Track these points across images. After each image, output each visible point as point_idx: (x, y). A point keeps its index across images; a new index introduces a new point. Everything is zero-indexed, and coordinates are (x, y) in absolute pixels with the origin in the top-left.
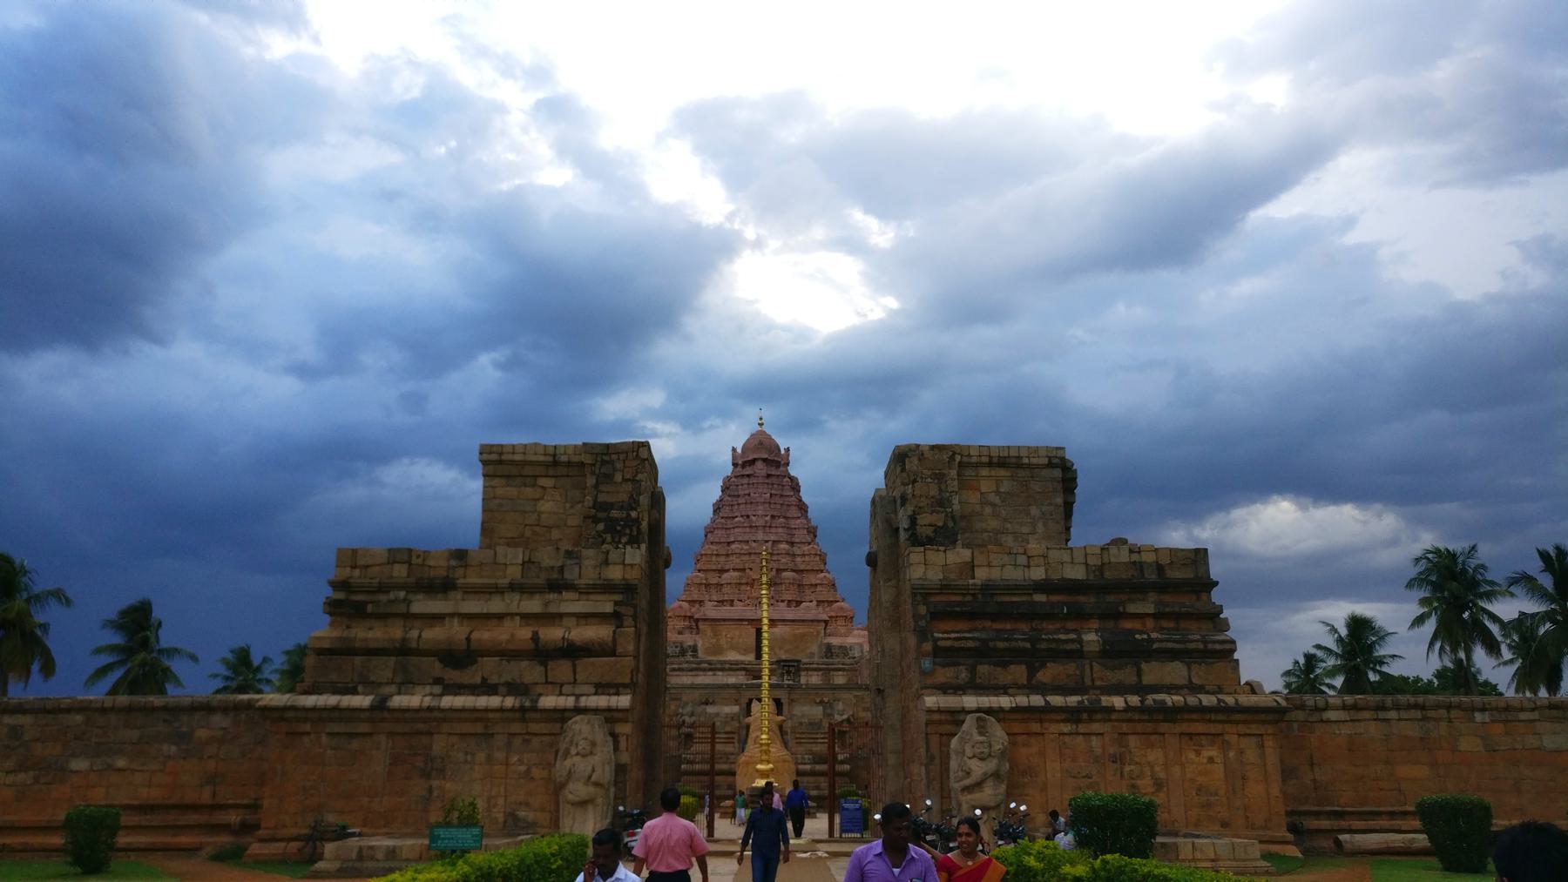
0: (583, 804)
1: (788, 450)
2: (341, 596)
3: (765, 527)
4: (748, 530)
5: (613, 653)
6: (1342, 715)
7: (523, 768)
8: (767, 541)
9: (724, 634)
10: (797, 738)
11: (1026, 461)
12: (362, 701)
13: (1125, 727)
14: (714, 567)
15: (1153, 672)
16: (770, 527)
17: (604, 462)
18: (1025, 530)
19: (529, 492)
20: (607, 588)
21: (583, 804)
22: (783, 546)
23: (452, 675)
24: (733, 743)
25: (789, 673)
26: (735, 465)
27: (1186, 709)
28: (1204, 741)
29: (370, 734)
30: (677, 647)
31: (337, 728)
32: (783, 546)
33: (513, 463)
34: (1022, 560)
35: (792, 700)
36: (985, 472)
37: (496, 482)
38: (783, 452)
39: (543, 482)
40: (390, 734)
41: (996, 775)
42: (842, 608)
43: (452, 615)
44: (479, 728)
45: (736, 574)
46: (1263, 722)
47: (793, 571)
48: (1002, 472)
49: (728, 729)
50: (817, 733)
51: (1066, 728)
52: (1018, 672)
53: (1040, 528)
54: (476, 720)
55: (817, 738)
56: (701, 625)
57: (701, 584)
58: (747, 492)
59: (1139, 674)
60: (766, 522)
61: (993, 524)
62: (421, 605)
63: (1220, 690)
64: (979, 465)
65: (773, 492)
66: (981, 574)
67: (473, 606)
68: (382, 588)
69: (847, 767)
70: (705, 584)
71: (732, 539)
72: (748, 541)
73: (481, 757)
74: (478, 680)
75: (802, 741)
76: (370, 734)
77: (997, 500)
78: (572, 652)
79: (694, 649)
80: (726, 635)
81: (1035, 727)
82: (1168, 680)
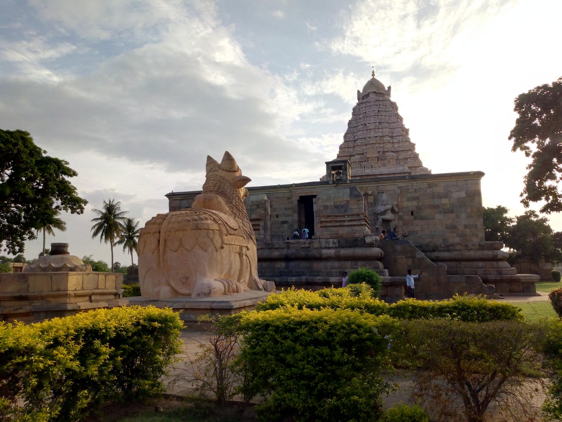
10: (321, 222)
16: (378, 129)
24: (259, 230)
26: (359, 99)
38: (387, 89)
50: (344, 216)
55: (344, 221)
58: (364, 111)
69: (376, 251)
71: (356, 138)
75: (328, 224)
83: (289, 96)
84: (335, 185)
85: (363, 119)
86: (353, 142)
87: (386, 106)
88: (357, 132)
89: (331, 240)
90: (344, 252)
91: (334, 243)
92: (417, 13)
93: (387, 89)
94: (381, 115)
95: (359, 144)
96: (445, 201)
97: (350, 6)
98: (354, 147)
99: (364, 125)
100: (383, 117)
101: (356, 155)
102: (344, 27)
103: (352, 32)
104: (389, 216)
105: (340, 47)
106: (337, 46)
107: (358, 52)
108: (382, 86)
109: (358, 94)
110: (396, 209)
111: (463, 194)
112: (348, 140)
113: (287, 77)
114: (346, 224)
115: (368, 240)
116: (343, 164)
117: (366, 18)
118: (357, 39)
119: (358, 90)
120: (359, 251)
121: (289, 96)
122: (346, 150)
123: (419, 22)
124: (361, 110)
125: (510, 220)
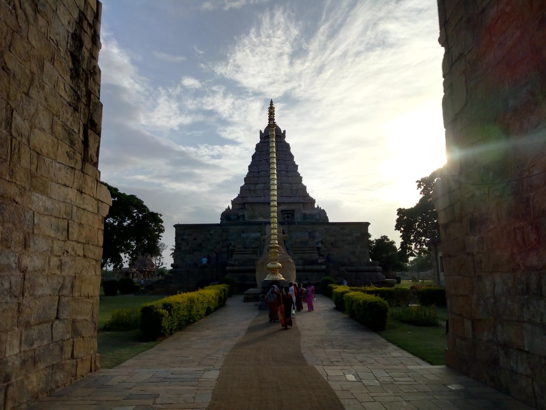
1: (285, 131)
14: (252, 182)
25: (288, 217)
26: (261, 138)
30: (235, 216)
35: (290, 231)
38: (282, 132)
49: (254, 246)
55: (305, 250)
56: (246, 206)
57: (246, 190)
58: (266, 149)
69: (324, 267)
70: (249, 190)
71: (260, 170)
72: (267, 171)
75: (298, 252)
79: (243, 216)
80: (258, 210)
83: (170, 108)
84: (289, 225)
85: (265, 155)
86: (257, 172)
87: (283, 146)
88: (261, 165)
89: (299, 261)
90: (307, 267)
91: (301, 263)
92: (291, 53)
93: (282, 132)
94: (279, 154)
95: (262, 175)
96: (349, 238)
97: (235, 38)
98: (258, 177)
99: (266, 160)
100: (281, 155)
101: (285, 197)
102: (228, 55)
103: (235, 60)
104: (320, 245)
105: (223, 71)
106: (220, 70)
107: (239, 77)
108: (280, 130)
109: (260, 134)
110: (324, 241)
111: (359, 235)
112: (253, 171)
113: (170, 90)
114: (307, 252)
115: (319, 261)
116: (292, 212)
117: (248, 51)
118: (238, 67)
119: (260, 130)
120: (315, 267)
121: (170, 108)
122: (252, 178)
123: (292, 59)
124: (263, 147)
125: (372, 242)
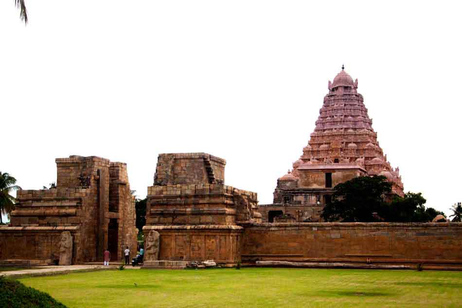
0: (64, 252)
1: (357, 80)
2: (18, 202)
3: (341, 121)
4: (333, 123)
5: (76, 216)
6: (276, 229)
7: (55, 244)
8: (342, 129)
9: (311, 176)
11: (193, 157)
12: (20, 228)
13: (191, 234)
14: (316, 142)
15: (204, 219)
17: (84, 162)
18: (192, 177)
19: (68, 171)
20: (75, 199)
21: (64, 252)
22: (351, 131)
23: (41, 221)
27: (205, 229)
28: (212, 237)
29: (23, 236)
31: (16, 235)
32: (351, 131)
33: (63, 163)
34: (175, 189)
36: (182, 161)
37: (60, 168)
38: (354, 81)
39: (72, 168)
40: (27, 236)
41: (154, 246)
42: (376, 161)
43: (42, 206)
44: (44, 234)
45: (326, 146)
46: (225, 232)
47: (354, 143)
48: (187, 161)
51: (177, 234)
52: (170, 219)
53: (196, 177)
54: (43, 233)
57: (309, 151)
58: (333, 104)
59: (200, 220)
60: (341, 119)
61: (184, 176)
62: (35, 204)
63: (219, 224)
64: (180, 159)
65: (346, 103)
66: (165, 193)
67: (46, 204)
68: (27, 200)
72: (332, 129)
73: (46, 241)
74: (46, 223)
76: (23, 236)
77: (185, 169)
78: (67, 215)
81: (170, 234)
82: (208, 221)
